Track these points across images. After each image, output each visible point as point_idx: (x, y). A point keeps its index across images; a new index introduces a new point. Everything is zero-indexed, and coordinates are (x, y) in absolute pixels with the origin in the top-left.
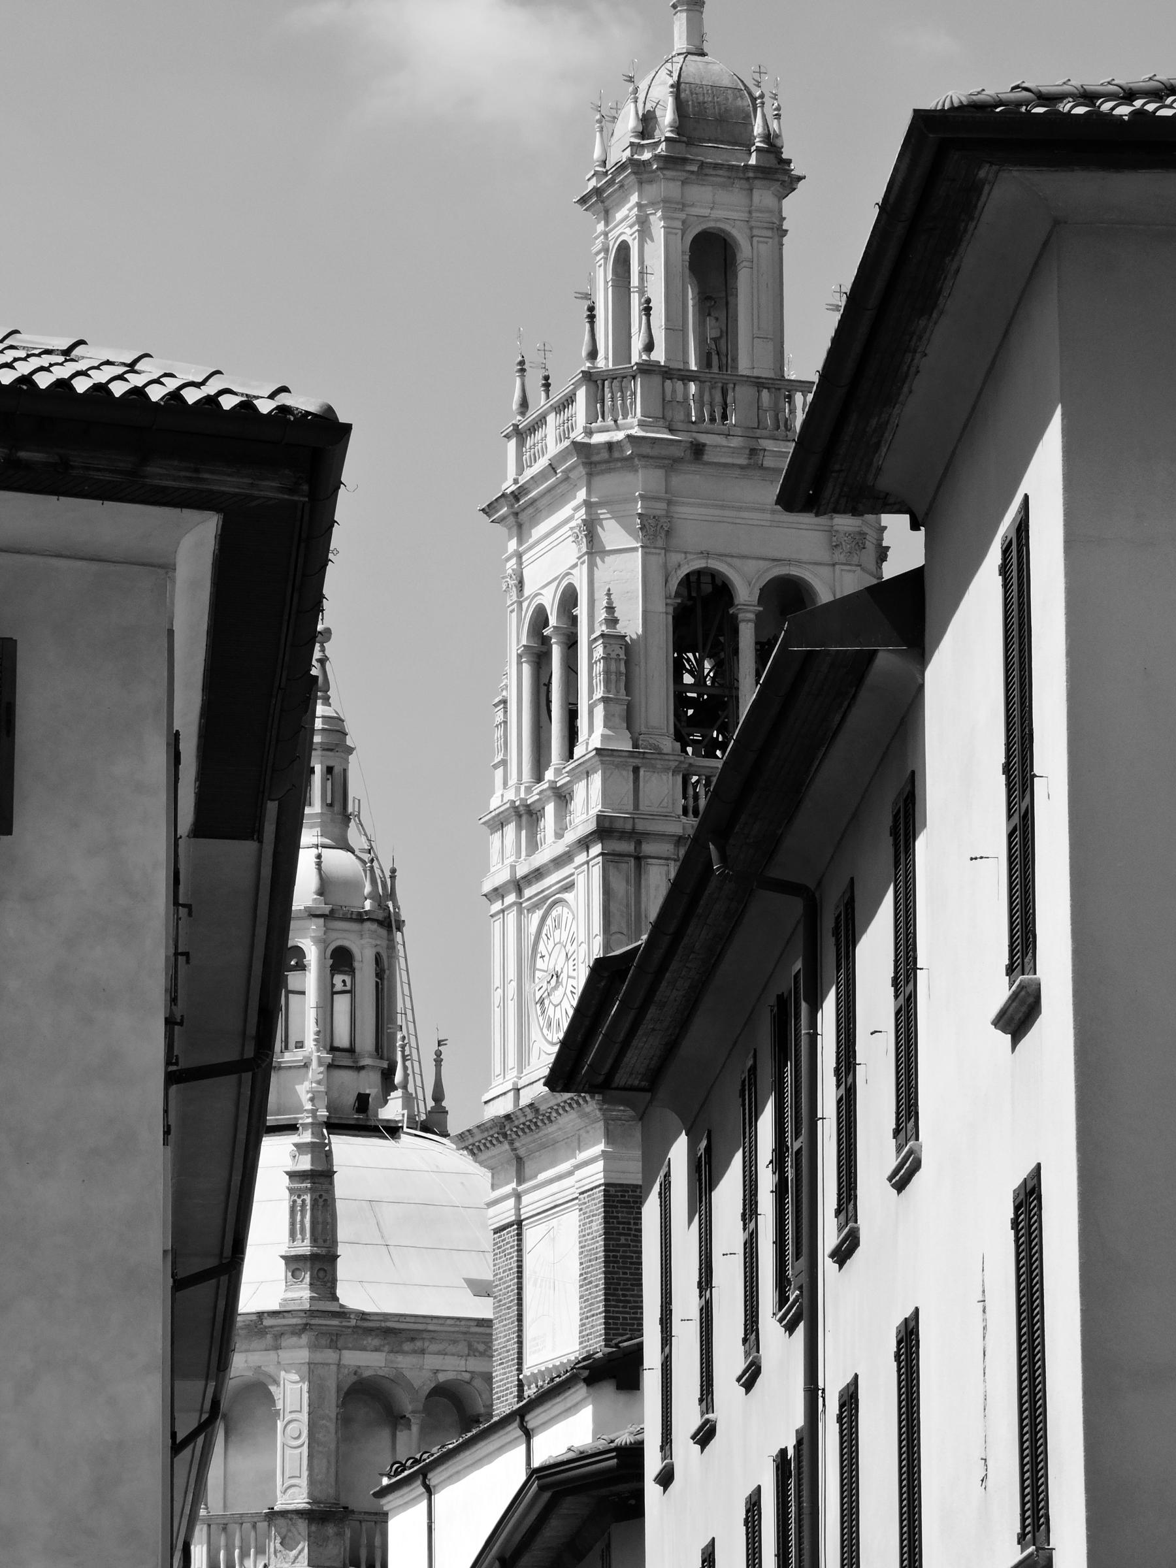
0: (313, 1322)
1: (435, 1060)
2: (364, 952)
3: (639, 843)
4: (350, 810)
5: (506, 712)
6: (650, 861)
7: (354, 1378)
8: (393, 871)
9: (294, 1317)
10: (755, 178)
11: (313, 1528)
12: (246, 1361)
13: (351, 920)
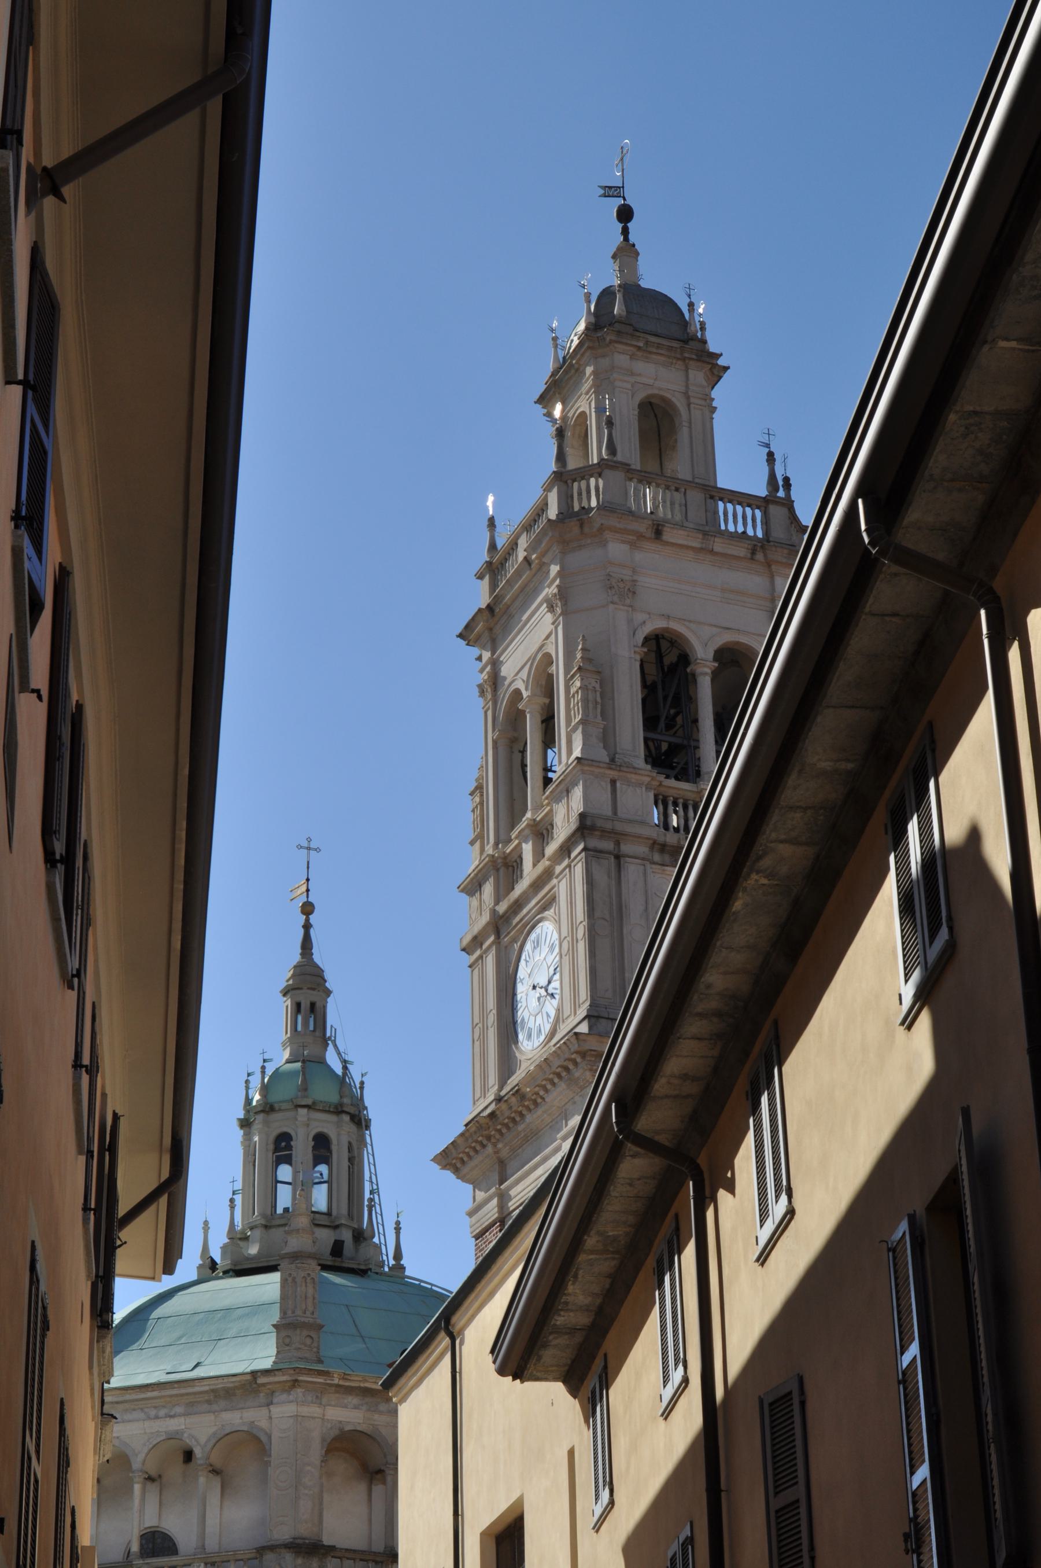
0: (301, 1378)
1: (395, 1228)
2: (339, 1132)
3: (618, 843)
4: (328, 1034)
5: (482, 795)
6: (627, 859)
7: (337, 1432)
8: (362, 1083)
9: (284, 1375)
10: (691, 359)
11: (299, 1561)
12: (241, 1418)
13: (329, 1112)
